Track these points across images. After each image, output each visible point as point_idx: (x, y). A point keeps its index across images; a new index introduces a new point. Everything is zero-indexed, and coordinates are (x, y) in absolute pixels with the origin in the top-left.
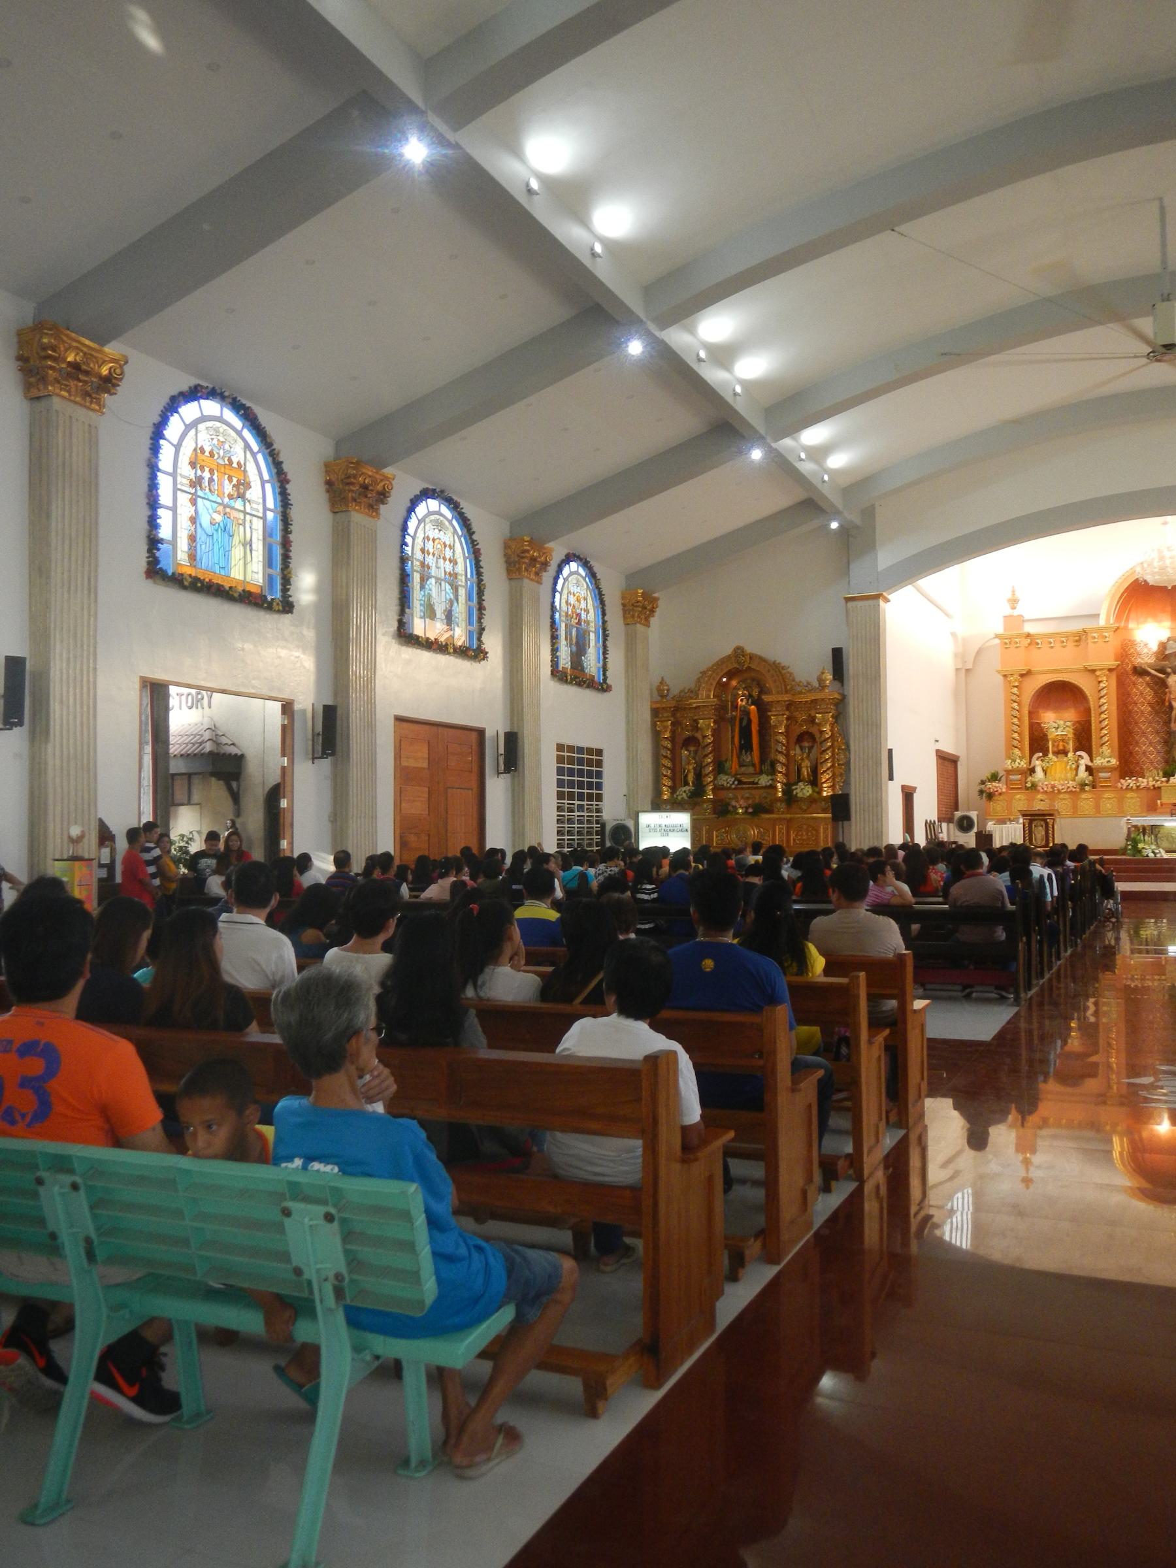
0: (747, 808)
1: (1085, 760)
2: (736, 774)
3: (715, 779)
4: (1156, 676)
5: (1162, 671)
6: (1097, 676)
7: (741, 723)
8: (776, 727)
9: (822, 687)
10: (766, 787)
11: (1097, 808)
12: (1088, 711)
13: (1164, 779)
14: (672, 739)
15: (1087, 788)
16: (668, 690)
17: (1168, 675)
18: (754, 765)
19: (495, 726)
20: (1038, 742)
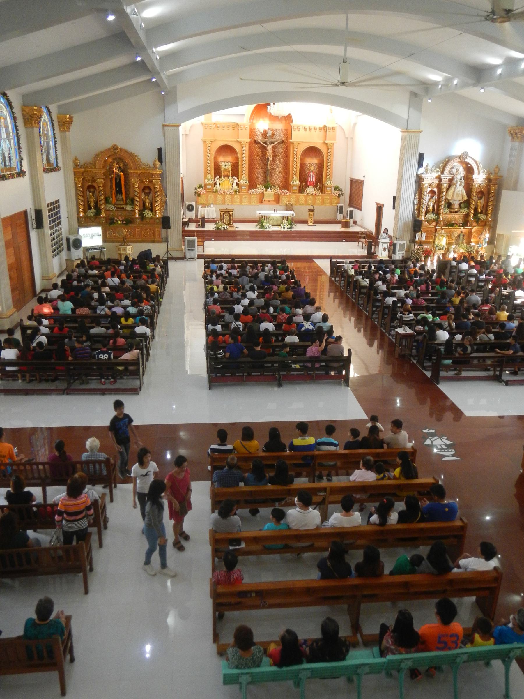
0: (123, 221)
1: (236, 181)
2: (115, 204)
3: (105, 206)
4: (261, 144)
5: (265, 143)
6: (241, 145)
7: (116, 179)
8: (134, 184)
9: (155, 166)
10: (130, 211)
11: (241, 201)
12: (237, 158)
13: (265, 189)
14: (82, 187)
15: (237, 193)
16: (79, 163)
17: (268, 145)
18: (123, 200)
19: (29, 207)
20: (217, 171)
